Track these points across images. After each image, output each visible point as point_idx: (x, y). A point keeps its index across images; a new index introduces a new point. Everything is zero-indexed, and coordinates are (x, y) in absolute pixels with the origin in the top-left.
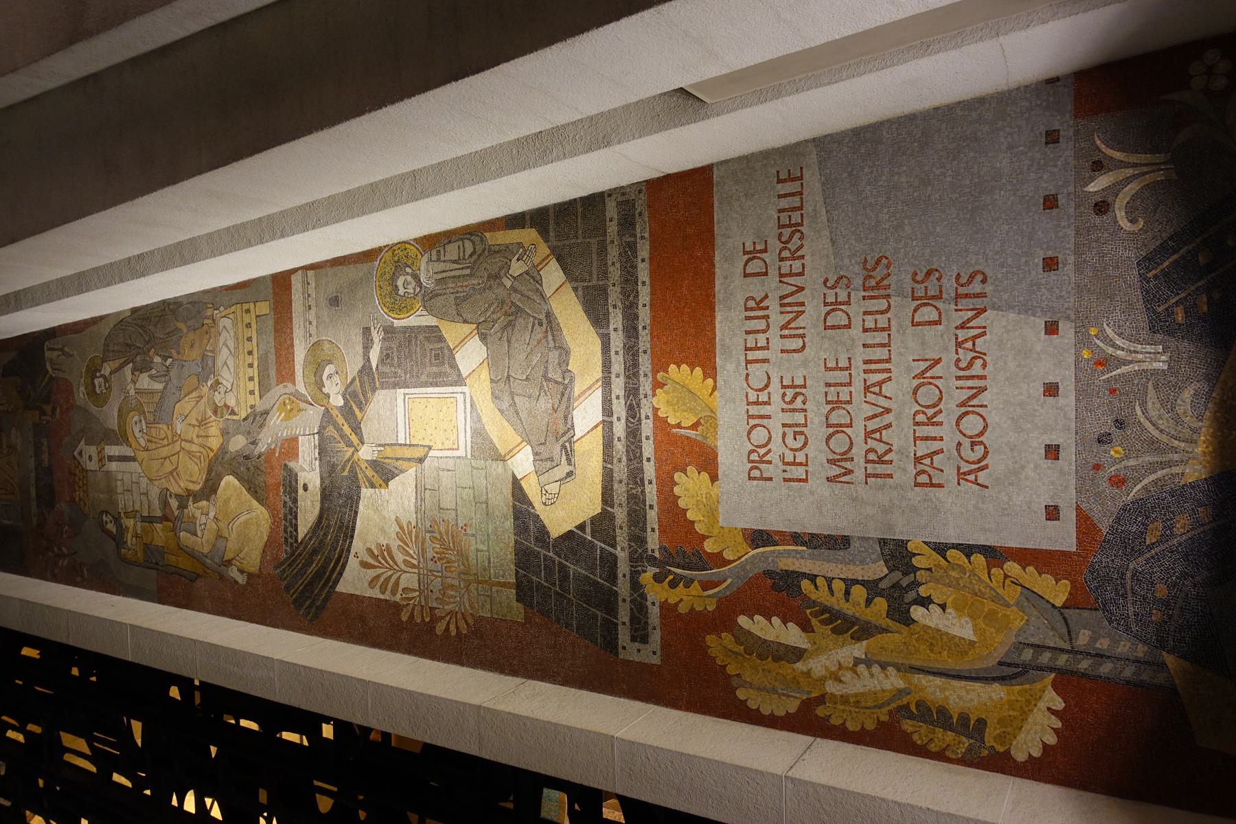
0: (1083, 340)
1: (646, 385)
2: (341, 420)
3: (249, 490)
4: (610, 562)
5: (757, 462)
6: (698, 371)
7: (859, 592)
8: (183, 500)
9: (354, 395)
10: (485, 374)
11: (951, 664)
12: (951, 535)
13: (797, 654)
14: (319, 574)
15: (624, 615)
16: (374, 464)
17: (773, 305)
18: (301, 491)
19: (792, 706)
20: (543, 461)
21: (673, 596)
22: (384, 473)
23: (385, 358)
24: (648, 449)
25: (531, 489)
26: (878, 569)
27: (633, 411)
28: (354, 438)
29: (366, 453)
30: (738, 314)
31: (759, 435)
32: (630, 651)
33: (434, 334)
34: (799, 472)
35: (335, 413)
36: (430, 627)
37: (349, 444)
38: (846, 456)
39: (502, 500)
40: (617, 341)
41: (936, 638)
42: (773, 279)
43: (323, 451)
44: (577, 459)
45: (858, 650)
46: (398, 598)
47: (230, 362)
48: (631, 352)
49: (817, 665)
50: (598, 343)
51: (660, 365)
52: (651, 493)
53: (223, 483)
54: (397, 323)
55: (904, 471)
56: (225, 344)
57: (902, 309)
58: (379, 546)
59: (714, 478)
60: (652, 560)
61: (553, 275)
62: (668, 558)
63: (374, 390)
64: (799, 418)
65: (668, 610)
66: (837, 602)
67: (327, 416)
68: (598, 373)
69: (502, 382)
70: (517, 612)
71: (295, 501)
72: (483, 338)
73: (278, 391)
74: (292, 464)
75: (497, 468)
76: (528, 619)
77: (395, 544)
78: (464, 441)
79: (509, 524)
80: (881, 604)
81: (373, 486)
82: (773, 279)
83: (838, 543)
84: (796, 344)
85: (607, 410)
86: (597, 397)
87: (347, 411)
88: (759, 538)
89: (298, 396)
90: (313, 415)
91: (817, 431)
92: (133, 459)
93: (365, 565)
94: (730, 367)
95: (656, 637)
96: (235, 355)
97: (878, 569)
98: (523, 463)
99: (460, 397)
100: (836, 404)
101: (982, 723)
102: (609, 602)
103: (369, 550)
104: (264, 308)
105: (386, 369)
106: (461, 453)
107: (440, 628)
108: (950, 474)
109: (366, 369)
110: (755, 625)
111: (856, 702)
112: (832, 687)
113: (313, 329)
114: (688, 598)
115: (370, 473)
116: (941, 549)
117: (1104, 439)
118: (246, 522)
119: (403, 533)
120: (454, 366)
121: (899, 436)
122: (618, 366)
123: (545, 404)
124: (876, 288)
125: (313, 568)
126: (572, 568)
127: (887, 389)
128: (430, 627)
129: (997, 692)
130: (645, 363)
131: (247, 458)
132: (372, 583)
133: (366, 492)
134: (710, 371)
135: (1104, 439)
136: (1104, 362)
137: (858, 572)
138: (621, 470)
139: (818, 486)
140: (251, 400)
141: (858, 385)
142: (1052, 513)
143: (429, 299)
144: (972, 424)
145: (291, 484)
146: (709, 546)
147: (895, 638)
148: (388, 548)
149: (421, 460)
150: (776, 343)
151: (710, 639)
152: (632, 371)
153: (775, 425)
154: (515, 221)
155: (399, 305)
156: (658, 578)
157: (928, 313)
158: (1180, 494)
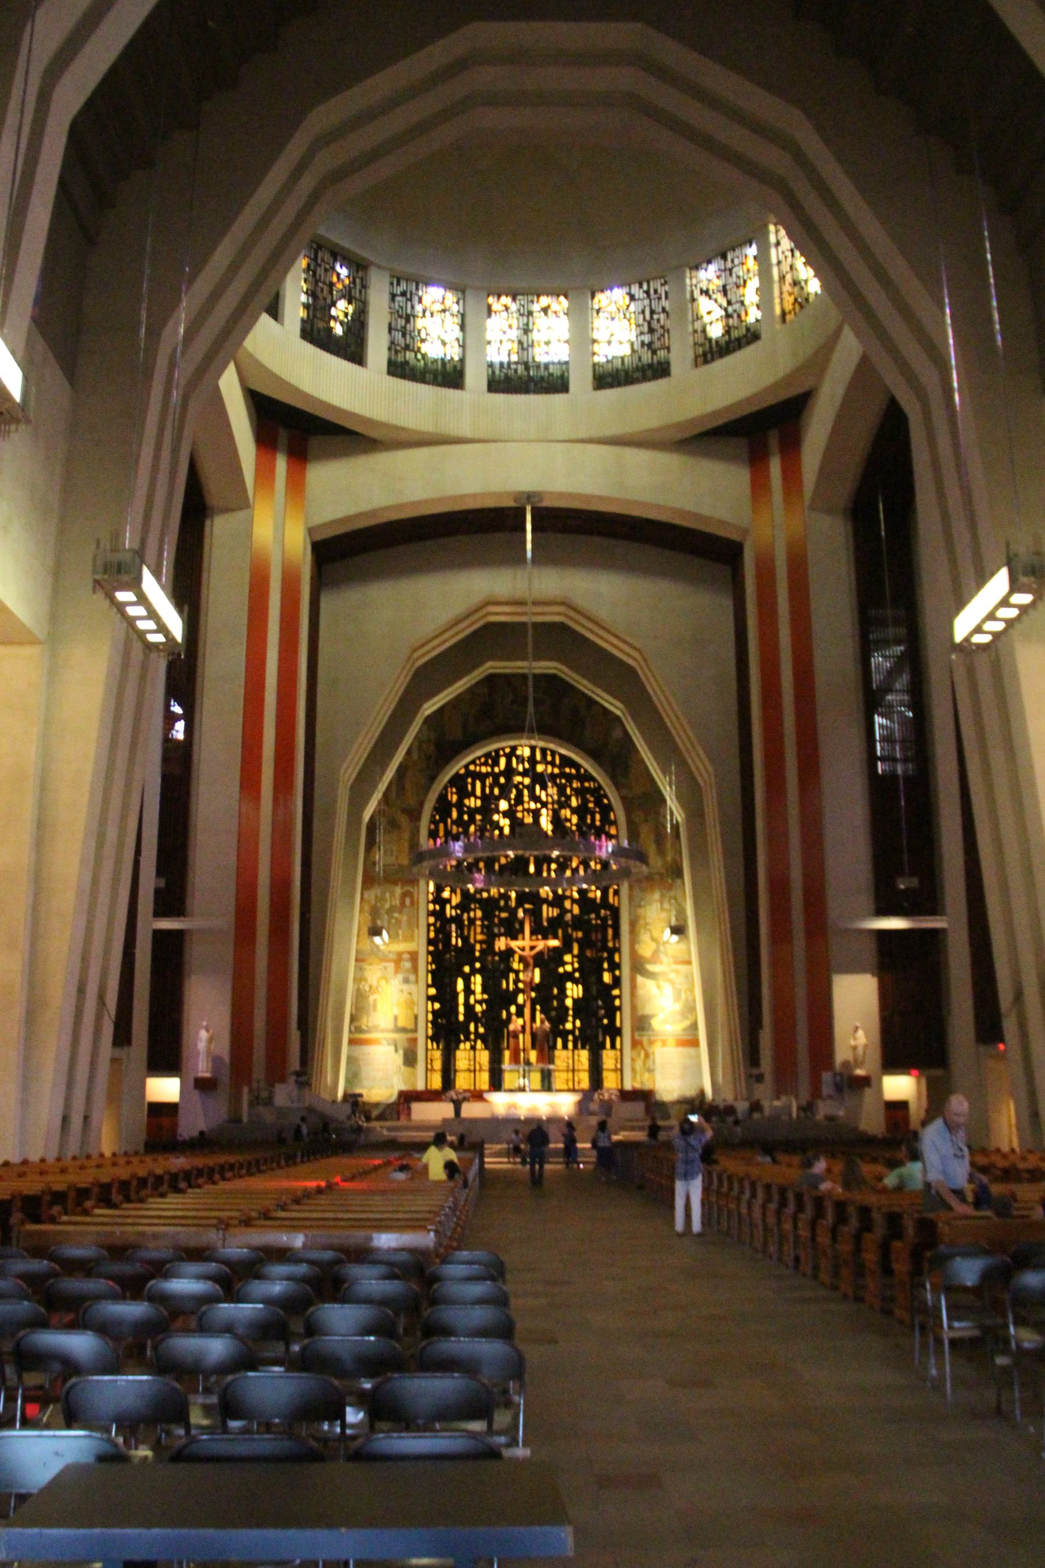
8: (650, 930)
22: (658, 986)
61: (687, 1023)
73: (671, 960)
83: (654, 1062)
88: (654, 1054)
104: (686, 958)
143: (687, 1000)
154: (696, 1016)
155: (686, 992)
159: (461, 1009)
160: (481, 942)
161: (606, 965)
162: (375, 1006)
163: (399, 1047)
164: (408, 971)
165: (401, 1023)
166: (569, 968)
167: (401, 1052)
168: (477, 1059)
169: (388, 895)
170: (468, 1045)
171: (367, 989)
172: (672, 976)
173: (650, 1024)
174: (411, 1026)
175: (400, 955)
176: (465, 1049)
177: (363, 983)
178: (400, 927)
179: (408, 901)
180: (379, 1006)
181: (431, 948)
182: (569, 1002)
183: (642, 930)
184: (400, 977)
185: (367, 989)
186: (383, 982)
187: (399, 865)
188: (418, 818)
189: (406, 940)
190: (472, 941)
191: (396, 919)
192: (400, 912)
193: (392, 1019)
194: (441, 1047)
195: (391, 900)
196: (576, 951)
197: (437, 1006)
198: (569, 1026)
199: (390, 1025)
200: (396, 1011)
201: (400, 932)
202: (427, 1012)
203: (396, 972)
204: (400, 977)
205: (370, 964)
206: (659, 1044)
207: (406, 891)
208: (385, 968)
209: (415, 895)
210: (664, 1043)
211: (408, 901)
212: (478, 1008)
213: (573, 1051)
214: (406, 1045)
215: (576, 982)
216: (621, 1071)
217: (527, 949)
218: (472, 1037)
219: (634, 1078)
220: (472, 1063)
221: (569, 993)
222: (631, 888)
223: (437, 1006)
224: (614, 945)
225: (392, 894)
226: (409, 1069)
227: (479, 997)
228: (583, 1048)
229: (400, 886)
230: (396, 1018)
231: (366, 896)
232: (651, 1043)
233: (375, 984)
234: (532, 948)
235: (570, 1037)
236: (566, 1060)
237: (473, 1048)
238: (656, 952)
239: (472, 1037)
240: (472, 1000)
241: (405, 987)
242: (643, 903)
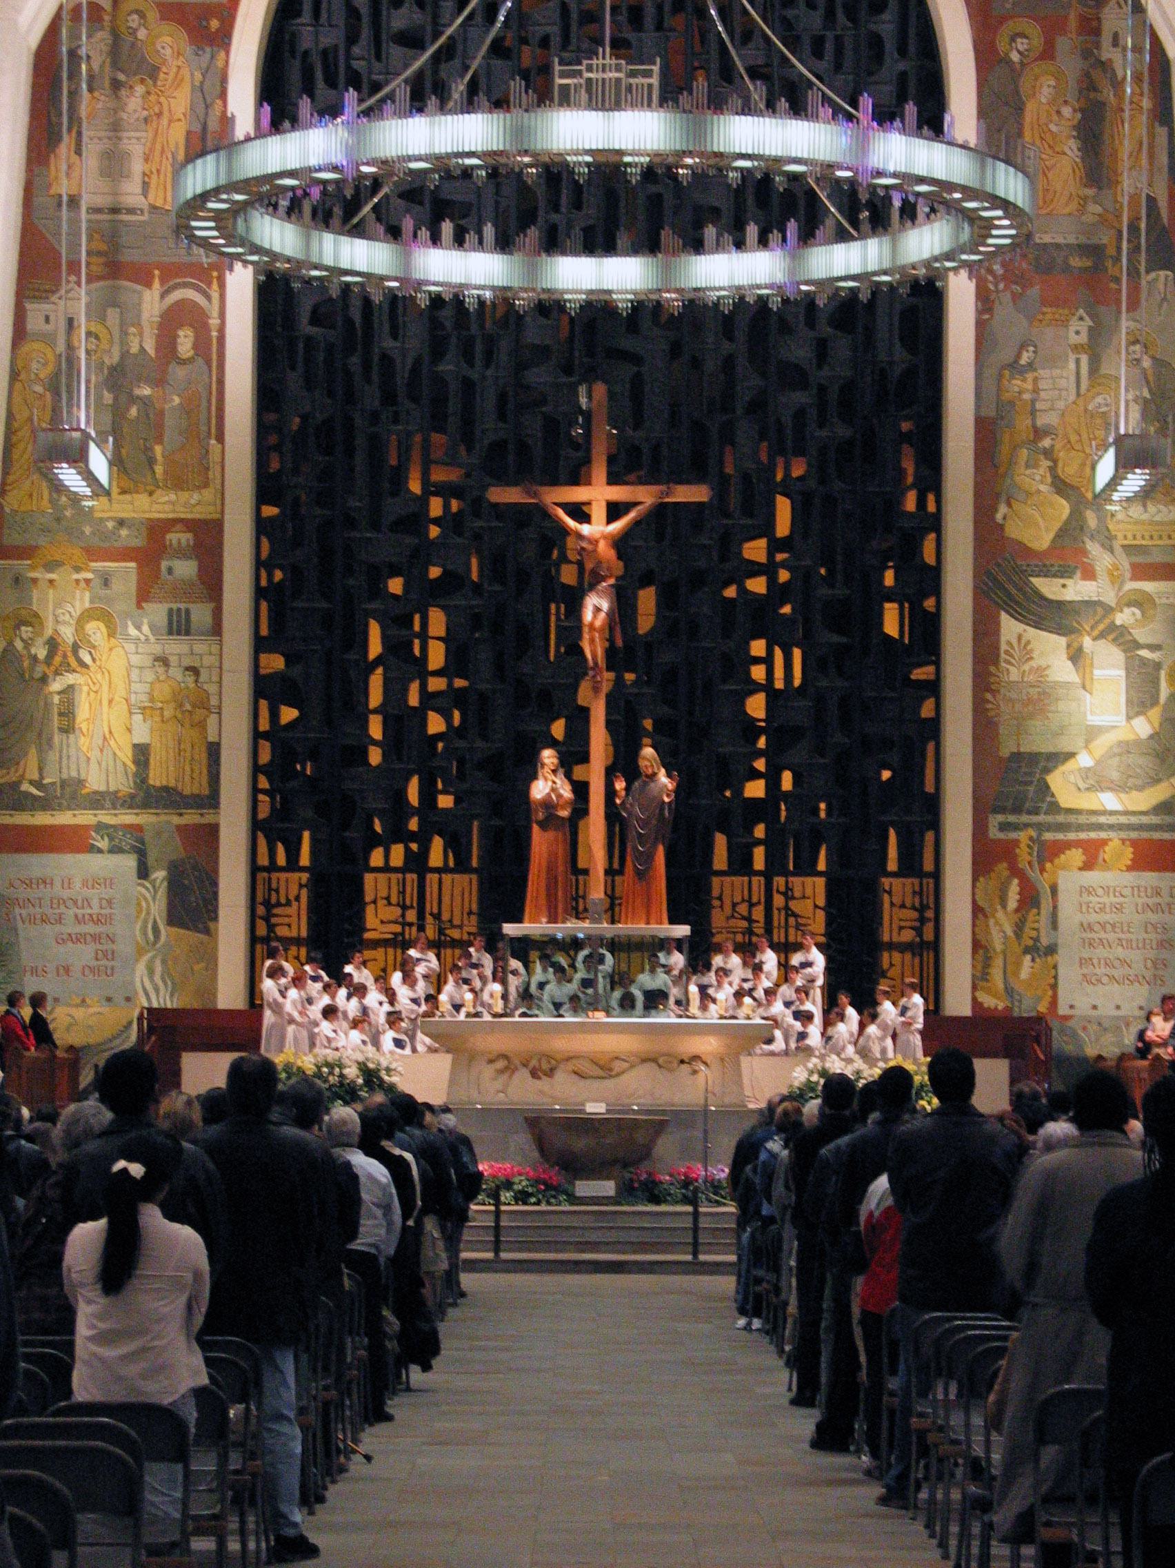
0: (1135, 1018)
1: (1123, 835)
2: (1107, 621)
3: (1061, 529)
4: (1036, 811)
5: (1089, 890)
6: (1129, 863)
7: (1034, 934)
9: (1122, 635)
10: (1131, 737)
11: (1009, 968)
12: (1061, 971)
13: (1004, 907)
14: (1009, 595)
15: (1012, 818)
16: (1080, 649)
17: (1158, 900)
18: (1062, 581)
19: (980, 903)
20: (1086, 773)
21: (1023, 845)
22: (1076, 656)
23: (1142, 659)
24: (1093, 835)
25: (1070, 765)
26: (1045, 941)
27: (1111, 827)
28: (1096, 633)
29: (1087, 642)
30: (1155, 883)
31: (1100, 892)
32: (995, 820)
33: (1155, 701)
34: (1084, 910)
35: (1111, 617)
36: (989, 690)
37: (1092, 628)
38: (1092, 930)
39: (1064, 745)
40: (1145, 820)
41: (1018, 964)
42: (1168, 899)
43: (1089, 604)
44: (1087, 794)
45: (1009, 932)
46: (1003, 664)
47: (1145, 517)
48: (1141, 827)
49: (1000, 914)
50: (1143, 808)
51: (1134, 843)
52: (1072, 836)
53: (1064, 502)
54: (1163, 674)
55: (1086, 954)
56: (1159, 511)
57: (1152, 954)
58: (1032, 651)
59: (1080, 869)
60: (1040, 835)
62: (1043, 844)
63: (1124, 651)
64: (1108, 910)
65: (1016, 843)
66: (1029, 925)
67: (1109, 610)
68: (1131, 808)
69: (1126, 748)
70: (1005, 752)
71: (1055, 576)
72: (1151, 737)
73: (1125, 564)
74: (1078, 574)
75: (1081, 743)
76: (1001, 759)
77: (1033, 663)
78: (1094, 720)
79: (1052, 749)
80: (1030, 943)
81: (1069, 646)
82: (1168, 899)
83: (1054, 925)
84: (1140, 908)
85: (1112, 813)
86: (1119, 807)
87: (1112, 627)
88: (1054, 890)
89: (1122, 583)
90: (1110, 598)
91: (1103, 917)
92: (1078, 394)
93: (1020, 638)
94: (1132, 879)
95: (1001, 836)
96: (1151, 523)
97: (1045, 941)
98: (1084, 760)
99: (1119, 718)
100: (1113, 926)
101: (987, 980)
102: (1017, 810)
103: (1028, 642)
105: (1137, 662)
106: (1089, 717)
107: (988, 696)
108: (1085, 971)
109: (1139, 646)
110: (1014, 888)
111: (988, 932)
112: (991, 922)
113: (1164, 601)
114: (1024, 856)
115: (1075, 645)
116: (1055, 967)
117: (1100, 1024)
118: (1037, 525)
119: (1040, 670)
120: (1138, 714)
121: (1101, 952)
122: (1134, 820)
123: (1115, 775)
124: (1161, 944)
125: (1014, 591)
126: (1031, 789)
127: (1120, 949)
128: (989, 690)
129: (1001, 986)
130: (1134, 835)
131: (1082, 529)
132: (1009, 643)
133: (1062, 641)
134: (1130, 869)
135: (1100, 1024)
136: (1127, 1025)
137: (1043, 933)
138: (1082, 819)
139: (1078, 917)
140: (1120, 536)
141: (1123, 936)
142: (1072, 1007)
144: (1105, 980)
145: (1065, 572)
146: (1048, 865)
147: (1018, 950)
148: (1031, 658)
149: (1084, 687)
150: (1140, 901)
151: (1005, 865)
152: (1130, 827)
153: (1105, 900)
156: (1031, 838)
157: (1149, 964)
158: (1081, 1047)
159: (376, 729)
160: (445, 491)
161: (889, 578)
162: (68, 713)
163: (151, 861)
164: (182, 591)
165: (157, 777)
166: (758, 585)
167: (160, 875)
168: (431, 906)
169: (113, 315)
170: (398, 854)
171: (42, 653)
172: (1121, 618)
173: (1045, 789)
174: (195, 785)
175: (157, 529)
176: (387, 869)
177: (26, 631)
178: (159, 439)
179: (185, 342)
180: (83, 713)
181: (270, 511)
182: (756, 706)
183: (1024, 453)
184: (158, 612)
185: (42, 653)
186: (95, 630)
187: (154, 208)
188: (223, 38)
189: (178, 483)
190: (415, 487)
191: (145, 402)
192: (160, 382)
193: (126, 756)
194: (305, 859)
195: (124, 333)
196: (783, 527)
197: (289, 714)
198: (755, 789)
199: (122, 783)
200: (142, 734)
201: (158, 449)
202: (257, 735)
203: (143, 596)
204: (158, 612)
205: (51, 566)
206: (1076, 856)
207: (180, 304)
208: (106, 583)
209: (214, 322)
210: (1092, 857)
211: (185, 342)
212: (435, 724)
213: (768, 875)
214: (176, 849)
215: (779, 637)
216: (935, 946)
217: (598, 512)
218: (413, 825)
219: (980, 979)
220: (411, 916)
221: (758, 673)
222: (985, 301)
223: (289, 714)
224: (921, 503)
225: (130, 319)
226: (194, 937)
227: (436, 684)
228: (806, 867)
229: (156, 284)
230: (142, 754)
231: (34, 323)
232: (1049, 852)
233: (68, 634)
234: (614, 511)
235: (760, 831)
236: (743, 909)
237: (417, 863)
238: (1071, 532)
239: (413, 825)
240: (414, 700)
241: (176, 647)
242: (1024, 360)
